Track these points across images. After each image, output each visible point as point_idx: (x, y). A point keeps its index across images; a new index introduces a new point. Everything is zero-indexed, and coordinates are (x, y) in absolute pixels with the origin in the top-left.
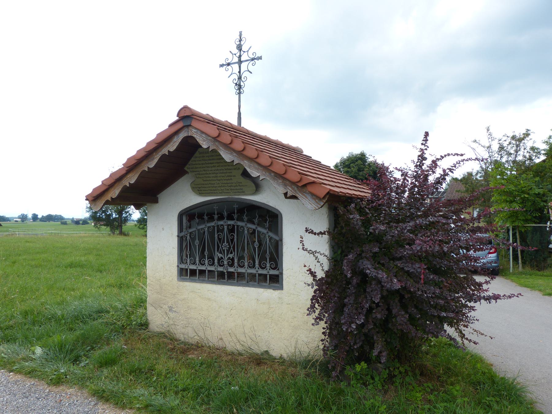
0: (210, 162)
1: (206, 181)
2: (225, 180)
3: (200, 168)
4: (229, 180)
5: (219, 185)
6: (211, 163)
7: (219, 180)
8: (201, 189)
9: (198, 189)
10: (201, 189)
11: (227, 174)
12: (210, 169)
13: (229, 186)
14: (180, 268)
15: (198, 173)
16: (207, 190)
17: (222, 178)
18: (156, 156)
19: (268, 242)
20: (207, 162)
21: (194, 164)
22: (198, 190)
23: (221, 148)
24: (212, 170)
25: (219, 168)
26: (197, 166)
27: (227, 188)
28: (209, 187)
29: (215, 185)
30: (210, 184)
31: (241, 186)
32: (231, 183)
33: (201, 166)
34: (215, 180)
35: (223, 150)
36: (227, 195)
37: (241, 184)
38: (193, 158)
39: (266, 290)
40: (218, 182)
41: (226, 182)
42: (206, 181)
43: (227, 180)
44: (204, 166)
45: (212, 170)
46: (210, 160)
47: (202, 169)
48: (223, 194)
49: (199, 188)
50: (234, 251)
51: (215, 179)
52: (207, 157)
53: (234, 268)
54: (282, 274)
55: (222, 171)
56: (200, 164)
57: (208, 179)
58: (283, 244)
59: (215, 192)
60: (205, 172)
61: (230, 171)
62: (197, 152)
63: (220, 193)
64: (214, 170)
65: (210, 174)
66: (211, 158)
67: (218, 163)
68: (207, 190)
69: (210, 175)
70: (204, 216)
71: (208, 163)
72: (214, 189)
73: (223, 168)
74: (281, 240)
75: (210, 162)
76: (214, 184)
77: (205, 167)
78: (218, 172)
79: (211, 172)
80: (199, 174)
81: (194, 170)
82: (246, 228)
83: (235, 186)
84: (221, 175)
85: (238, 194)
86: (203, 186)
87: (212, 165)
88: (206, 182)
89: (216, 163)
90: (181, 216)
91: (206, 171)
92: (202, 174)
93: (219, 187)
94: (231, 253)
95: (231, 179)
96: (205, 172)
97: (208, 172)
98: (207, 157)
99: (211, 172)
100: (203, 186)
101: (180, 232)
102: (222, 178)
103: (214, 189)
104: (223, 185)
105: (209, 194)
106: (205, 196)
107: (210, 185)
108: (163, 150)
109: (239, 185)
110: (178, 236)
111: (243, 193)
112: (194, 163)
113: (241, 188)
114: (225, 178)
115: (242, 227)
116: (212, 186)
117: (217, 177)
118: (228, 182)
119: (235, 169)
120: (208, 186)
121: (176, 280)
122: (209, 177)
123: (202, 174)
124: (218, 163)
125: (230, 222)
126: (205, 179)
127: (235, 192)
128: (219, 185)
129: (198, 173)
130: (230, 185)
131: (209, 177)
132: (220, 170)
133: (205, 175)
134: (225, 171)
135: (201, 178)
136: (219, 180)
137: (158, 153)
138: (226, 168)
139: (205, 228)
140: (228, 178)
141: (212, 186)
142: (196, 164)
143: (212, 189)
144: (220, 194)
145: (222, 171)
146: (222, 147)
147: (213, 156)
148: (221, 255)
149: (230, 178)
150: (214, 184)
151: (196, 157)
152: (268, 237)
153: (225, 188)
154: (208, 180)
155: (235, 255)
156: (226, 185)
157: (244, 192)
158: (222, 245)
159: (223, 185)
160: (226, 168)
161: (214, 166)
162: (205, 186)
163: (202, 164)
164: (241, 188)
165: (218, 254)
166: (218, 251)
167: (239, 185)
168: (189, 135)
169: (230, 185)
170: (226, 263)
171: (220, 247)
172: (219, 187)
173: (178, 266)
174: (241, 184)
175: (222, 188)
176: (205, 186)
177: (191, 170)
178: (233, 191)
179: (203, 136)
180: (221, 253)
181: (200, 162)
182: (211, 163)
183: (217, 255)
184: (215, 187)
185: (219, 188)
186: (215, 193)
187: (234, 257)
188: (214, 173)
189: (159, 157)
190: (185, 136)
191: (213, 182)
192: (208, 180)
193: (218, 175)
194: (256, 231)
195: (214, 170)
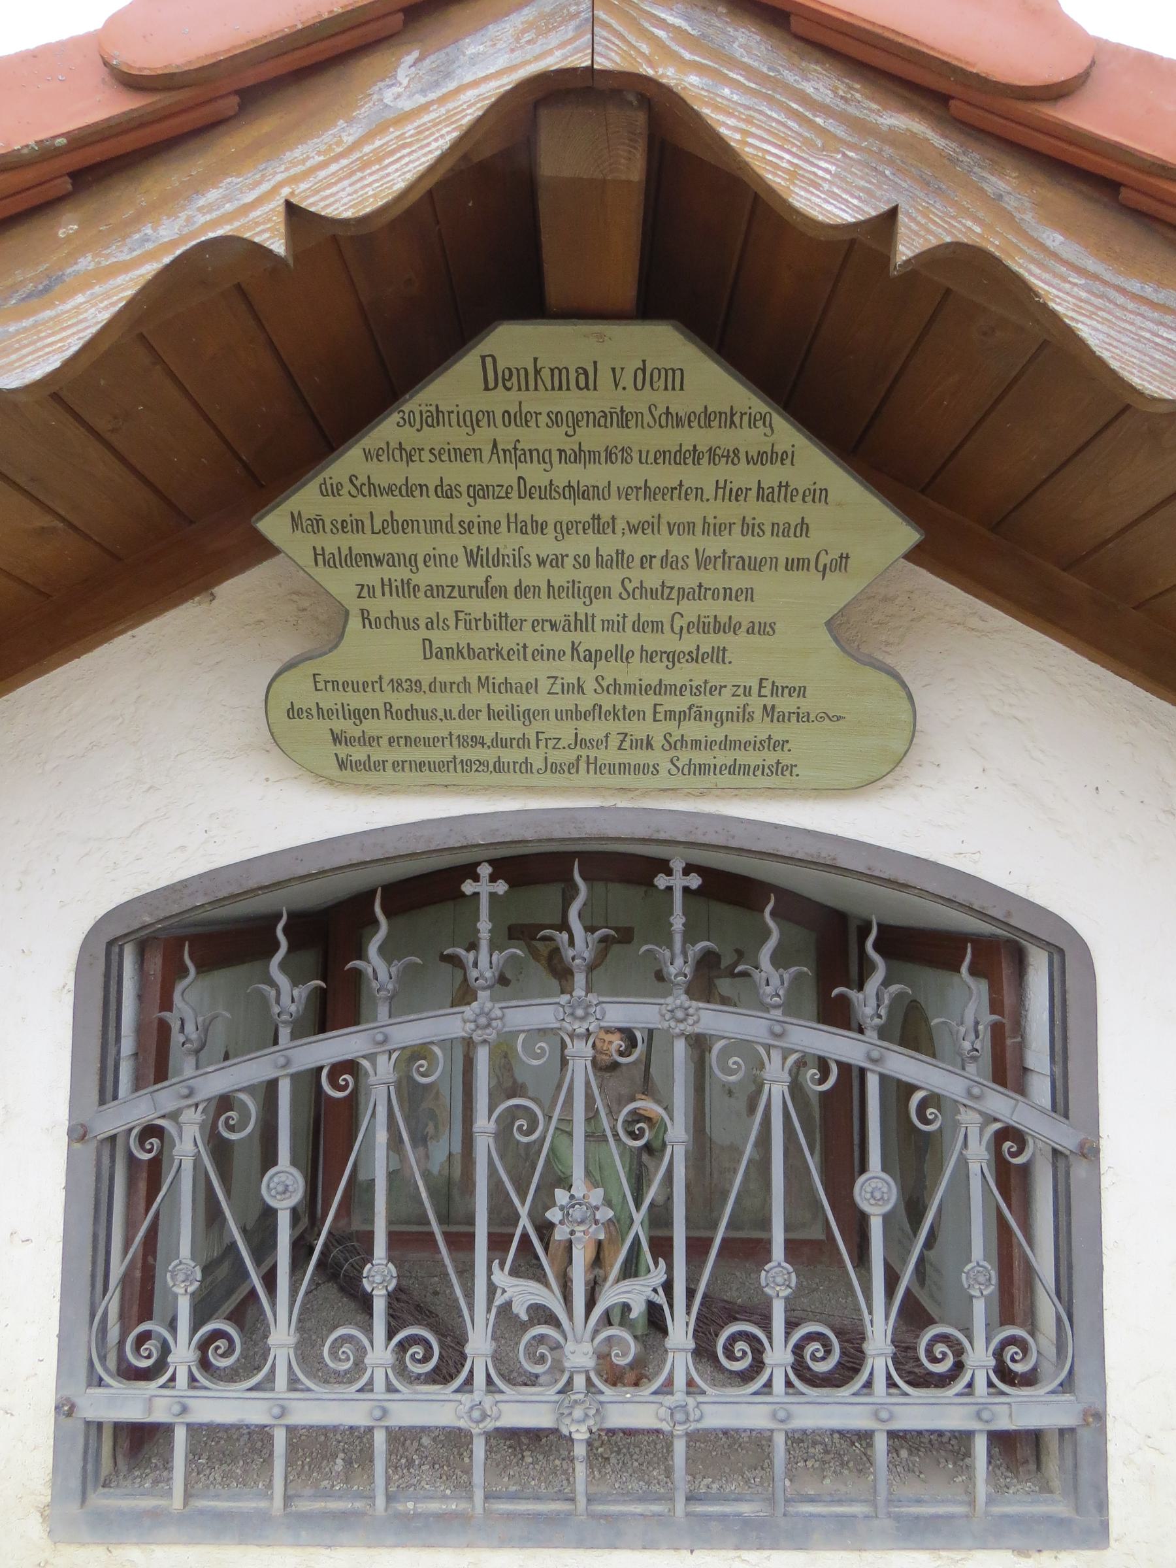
0: (564, 474)
1: (454, 653)
2: (649, 657)
3: (435, 526)
4: (695, 657)
5: (567, 702)
6: (576, 492)
7: (592, 657)
8: (371, 726)
9: (339, 725)
10: (371, 726)
11: (691, 610)
12: (542, 545)
13: (670, 715)
14: (88, 1423)
15: (399, 573)
16: (428, 742)
17: (632, 640)
18: (86, 263)
19: (974, 1168)
20: (535, 474)
21: (390, 491)
22: (336, 739)
23: (1054, 239)
24: (557, 561)
25: (637, 545)
26: (405, 508)
27: (638, 729)
28: (464, 713)
29: (526, 702)
30: (483, 683)
31: (783, 718)
32: (697, 691)
33: (460, 509)
34: (553, 655)
35: (1092, 264)
36: (595, 790)
37: (785, 704)
38: (396, 417)
39: (956, 1555)
40: (569, 670)
41: (653, 673)
42: (454, 653)
43: (673, 658)
44: (490, 509)
45: (557, 561)
46: (579, 456)
47: (452, 545)
48: (583, 778)
49: (359, 715)
50: (662, 1248)
51: (560, 641)
52: (555, 419)
53: (668, 1400)
54: (1097, 1417)
55: (652, 578)
56: (446, 492)
57: (482, 639)
58: (1105, 1181)
59: (510, 755)
60: (476, 576)
61: (737, 580)
62: (467, 366)
63: (556, 768)
64: (583, 562)
65: (522, 591)
66: (592, 438)
67: (649, 493)
68: (428, 742)
69: (516, 608)
70: (361, 954)
71: (549, 492)
72: (511, 729)
73: (681, 546)
74: (1090, 1152)
75: (564, 474)
76: (531, 687)
77: (490, 527)
78: (611, 578)
79: (535, 576)
80: (408, 589)
81: (363, 543)
82: (776, 1056)
83: (721, 719)
84: (632, 608)
85: (725, 779)
86: (402, 701)
87: (584, 510)
88: (447, 670)
89: (625, 493)
90: (116, 949)
91: (498, 560)
92: (436, 591)
93: (560, 715)
94: (631, 1269)
95: (719, 655)
96: (476, 576)
97: (504, 576)
98: (555, 419)
99: (535, 576)
100: (402, 701)
101: (107, 1093)
102: (632, 640)
103: (511, 729)
104: (608, 701)
105: (437, 778)
106: (393, 790)
107: (477, 700)
108: (213, 195)
109: (769, 711)
110: (78, 1133)
111: (775, 781)
112: (387, 473)
113: (779, 732)
114: (667, 642)
115: (743, 1046)
116: (500, 702)
117: (583, 624)
118: (681, 674)
119: (795, 564)
120: (453, 701)
121: (35, 1528)
122: (504, 622)
123: (436, 591)
124: (649, 493)
125: (619, 1013)
126: (441, 640)
127: (703, 769)
128: (567, 702)
129: (399, 573)
130: (679, 703)
131: (504, 622)
132: (646, 561)
133: (458, 604)
134: (687, 579)
135: (409, 624)
136: (592, 657)
137: (138, 219)
138: (713, 546)
139: (371, 1057)
140: (688, 643)
141: (500, 702)
142: (408, 490)
143: (484, 728)
144: (549, 779)
145: (652, 578)
146: (1067, 229)
147: (623, 419)
148: (533, 1286)
149: (708, 642)
150: (531, 687)
151: (436, 417)
152: (973, 1133)
153: (616, 727)
154: (472, 653)
155: (668, 1287)
156: (645, 703)
157: (780, 769)
158: (545, 1199)
159: (607, 701)
160: (713, 546)
161: (597, 525)
162: (423, 702)
163: (478, 492)
164: (779, 732)
165: (501, 1278)
166: (498, 1243)
167: (769, 711)
168: (602, 63)
169: (679, 703)
170: (589, 1362)
171: (525, 1222)
172: (560, 715)
173: (65, 1409)
174: (785, 704)
175: (592, 729)
176: (423, 702)
177: (331, 543)
178: (684, 756)
179: (804, 99)
180: (527, 1266)
181: (458, 474)
182: (576, 492)
183: (492, 1289)
184: (527, 716)
185: (565, 731)
186: (499, 767)
187: (661, 1299)
188: (574, 590)
189: (149, 269)
190: (554, 61)
191: (518, 671)
192: (472, 653)
193: (604, 609)
194: (873, 1083)
195: (583, 562)
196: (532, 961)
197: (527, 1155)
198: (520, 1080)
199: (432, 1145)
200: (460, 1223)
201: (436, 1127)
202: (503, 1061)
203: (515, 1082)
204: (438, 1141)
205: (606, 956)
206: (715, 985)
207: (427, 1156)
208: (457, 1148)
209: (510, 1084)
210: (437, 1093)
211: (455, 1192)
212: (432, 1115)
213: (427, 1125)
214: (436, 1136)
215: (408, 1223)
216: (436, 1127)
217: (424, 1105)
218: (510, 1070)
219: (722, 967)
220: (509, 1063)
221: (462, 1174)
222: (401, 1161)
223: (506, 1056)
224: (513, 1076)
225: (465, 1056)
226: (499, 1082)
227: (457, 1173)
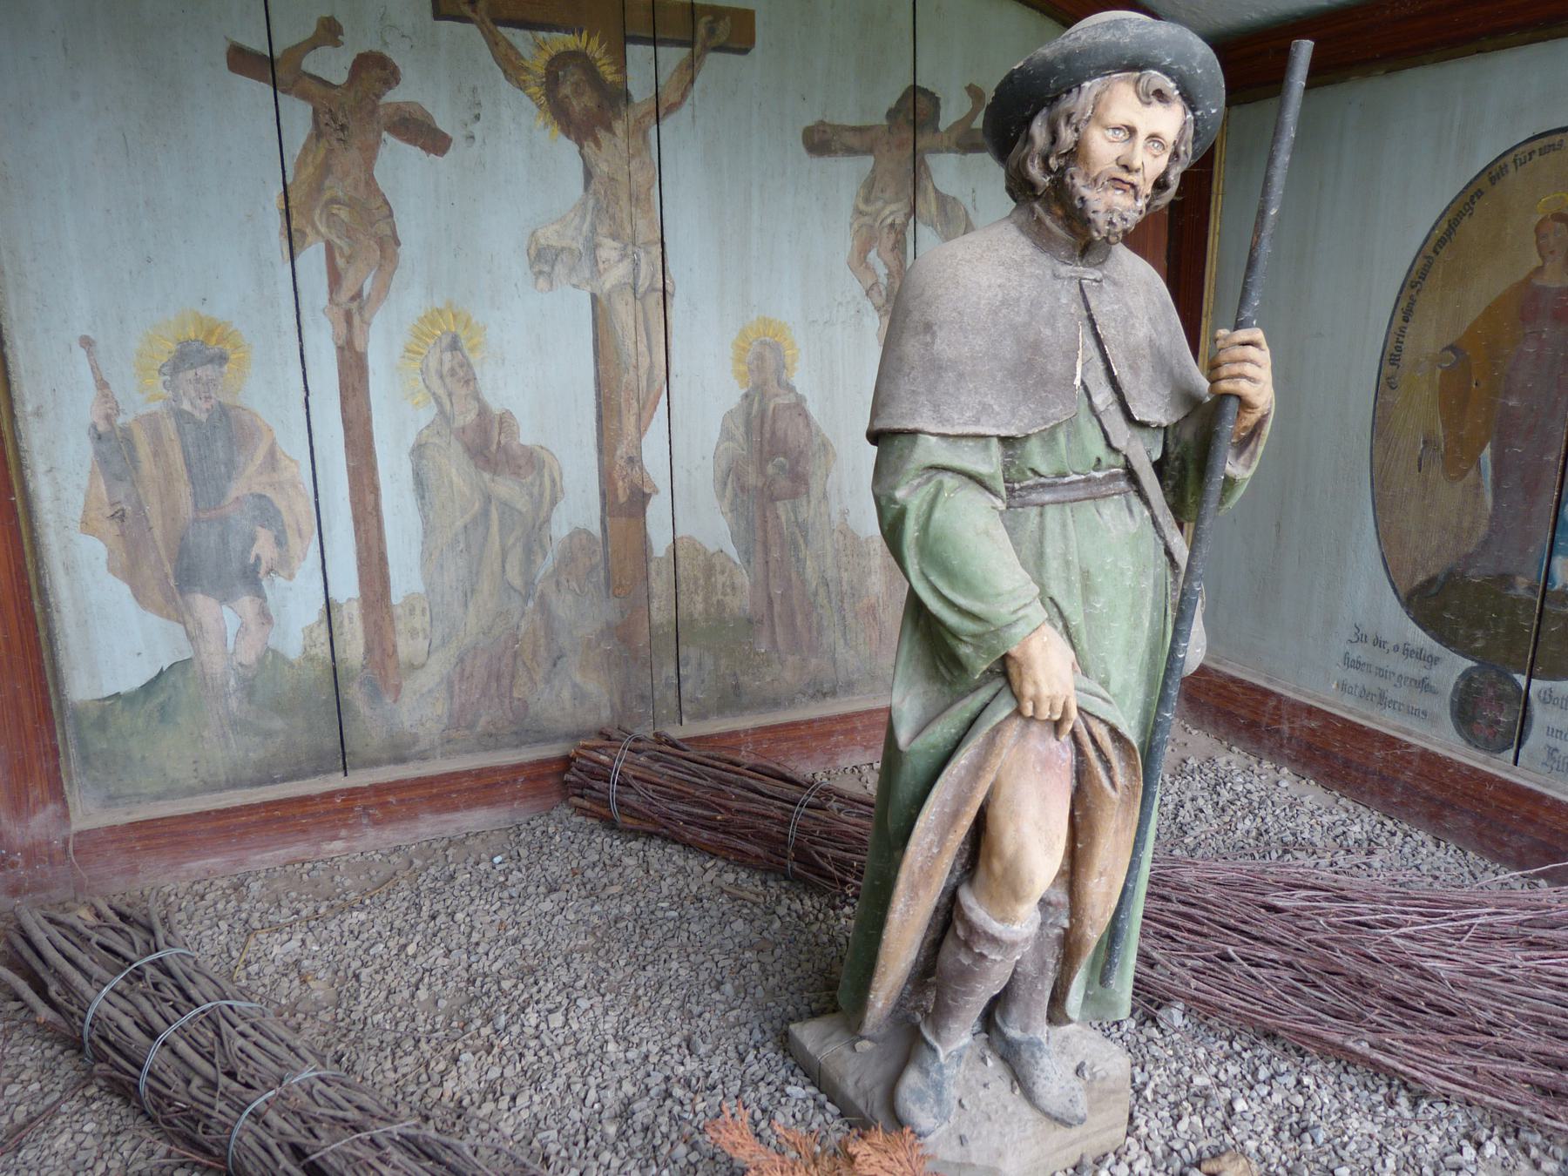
196: (506, 87)
197: (529, 584)
198: (496, 407)
199: (275, 586)
200: (376, 763)
201: (280, 542)
202: (447, 356)
203: (483, 411)
204: (291, 577)
205: (692, 81)
206: (927, 168)
207: (265, 617)
208: (347, 586)
209: (471, 417)
210: (272, 454)
211: (355, 694)
212: (266, 512)
213: (253, 539)
214: (284, 565)
215: (234, 784)
216: (280, 542)
217: (237, 489)
218: (469, 380)
219: (943, 125)
220: (466, 365)
221: (369, 650)
222: (191, 638)
223: (454, 345)
224: (477, 397)
225: (340, 349)
226: (442, 412)
227: (353, 648)
